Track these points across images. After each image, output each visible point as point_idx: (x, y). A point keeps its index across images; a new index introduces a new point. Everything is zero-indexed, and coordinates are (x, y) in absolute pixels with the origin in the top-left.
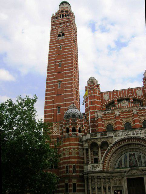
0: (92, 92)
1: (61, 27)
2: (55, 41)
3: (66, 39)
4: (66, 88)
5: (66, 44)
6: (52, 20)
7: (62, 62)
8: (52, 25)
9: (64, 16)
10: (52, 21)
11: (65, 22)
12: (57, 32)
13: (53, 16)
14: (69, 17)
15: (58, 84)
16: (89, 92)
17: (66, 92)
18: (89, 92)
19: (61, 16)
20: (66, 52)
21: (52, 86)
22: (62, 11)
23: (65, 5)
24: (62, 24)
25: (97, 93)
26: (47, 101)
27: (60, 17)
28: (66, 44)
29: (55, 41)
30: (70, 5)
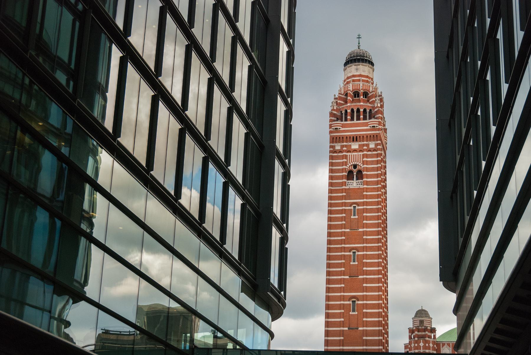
0: (422, 344)
1: (355, 151)
2: (342, 191)
3: (367, 190)
4: (367, 315)
5: (367, 204)
6: (331, 121)
7: (358, 251)
8: (334, 140)
9: (362, 117)
10: (331, 126)
11: (365, 137)
12: (346, 165)
13: (333, 110)
14: (373, 122)
15: (351, 302)
16: (416, 345)
17: (367, 324)
18: (416, 345)
19: (352, 110)
20: (367, 226)
21: (340, 307)
22: (356, 94)
23: (363, 69)
24: (357, 140)
25: (429, 348)
26: (329, 338)
27: (352, 119)
28: (367, 204)
29: (342, 191)
30: (372, 64)
